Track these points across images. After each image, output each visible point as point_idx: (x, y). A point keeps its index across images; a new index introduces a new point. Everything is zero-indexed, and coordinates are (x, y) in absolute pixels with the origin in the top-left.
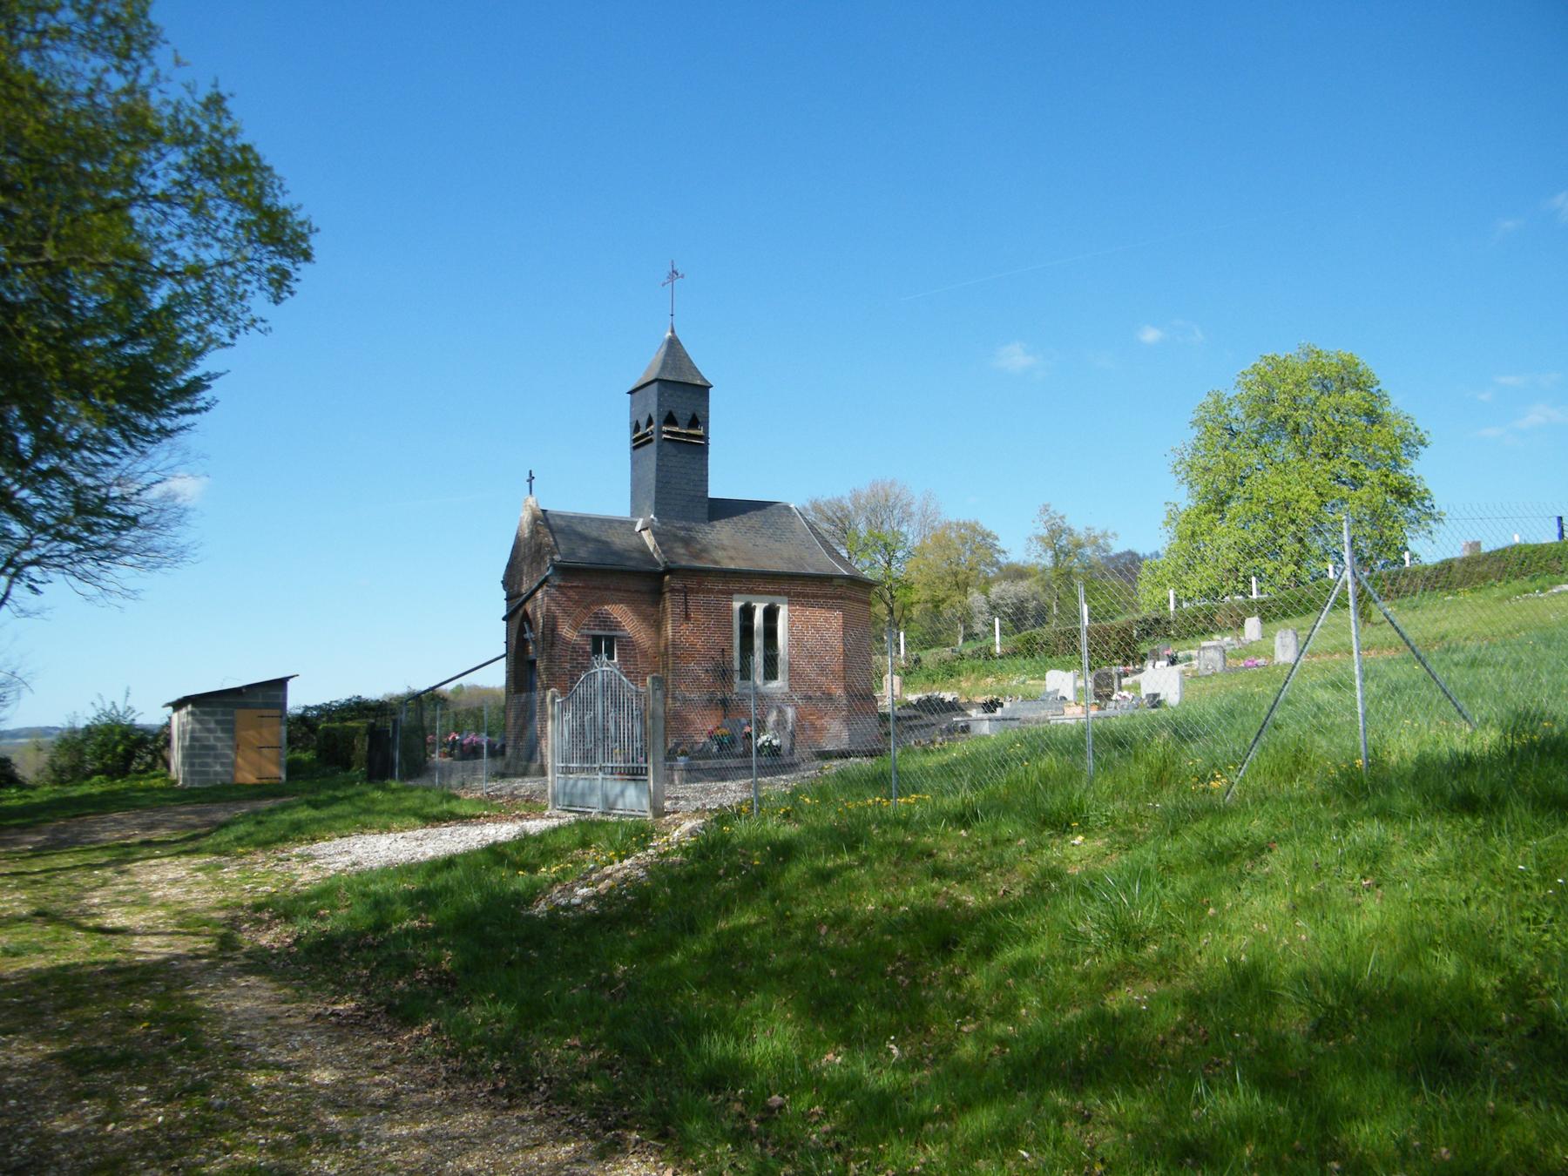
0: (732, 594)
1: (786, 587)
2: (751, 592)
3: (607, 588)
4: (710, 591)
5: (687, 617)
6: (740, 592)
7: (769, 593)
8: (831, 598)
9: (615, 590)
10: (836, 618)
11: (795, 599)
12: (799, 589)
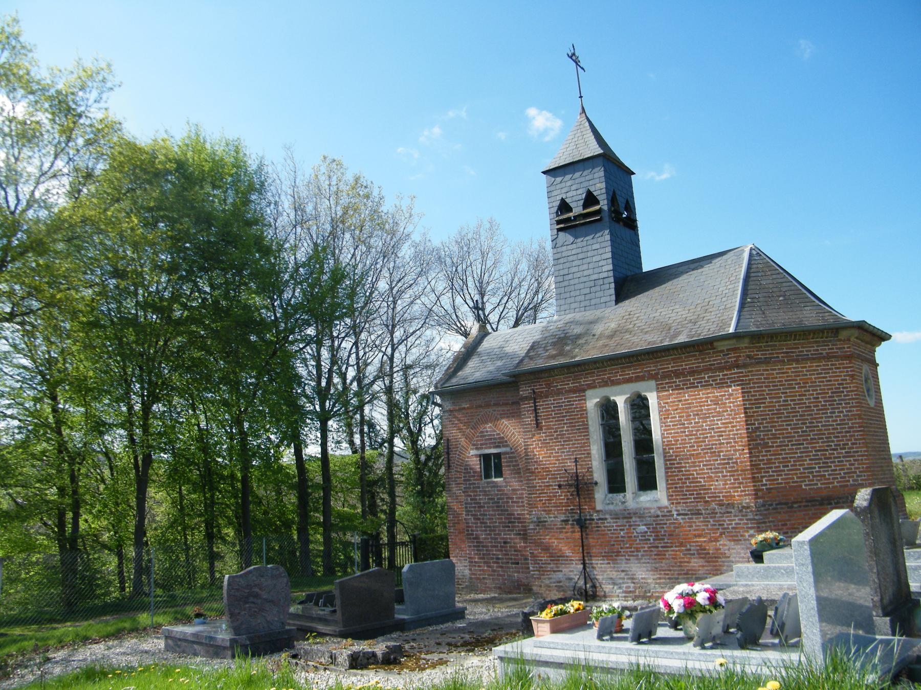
0: (584, 391)
1: (652, 368)
2: (606, 384)
3: (488, 405)
4: (559, 392)
5: (538, 426)
6: (592, 386)
7: (629, 381)
8: (721, 369)
9: (495, 405)
10: (733, 396)
11: (663, 381)
12: (670, 367)
